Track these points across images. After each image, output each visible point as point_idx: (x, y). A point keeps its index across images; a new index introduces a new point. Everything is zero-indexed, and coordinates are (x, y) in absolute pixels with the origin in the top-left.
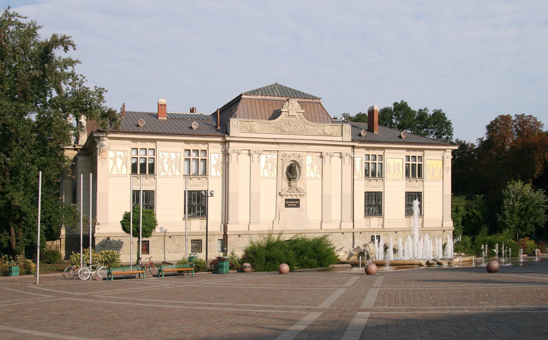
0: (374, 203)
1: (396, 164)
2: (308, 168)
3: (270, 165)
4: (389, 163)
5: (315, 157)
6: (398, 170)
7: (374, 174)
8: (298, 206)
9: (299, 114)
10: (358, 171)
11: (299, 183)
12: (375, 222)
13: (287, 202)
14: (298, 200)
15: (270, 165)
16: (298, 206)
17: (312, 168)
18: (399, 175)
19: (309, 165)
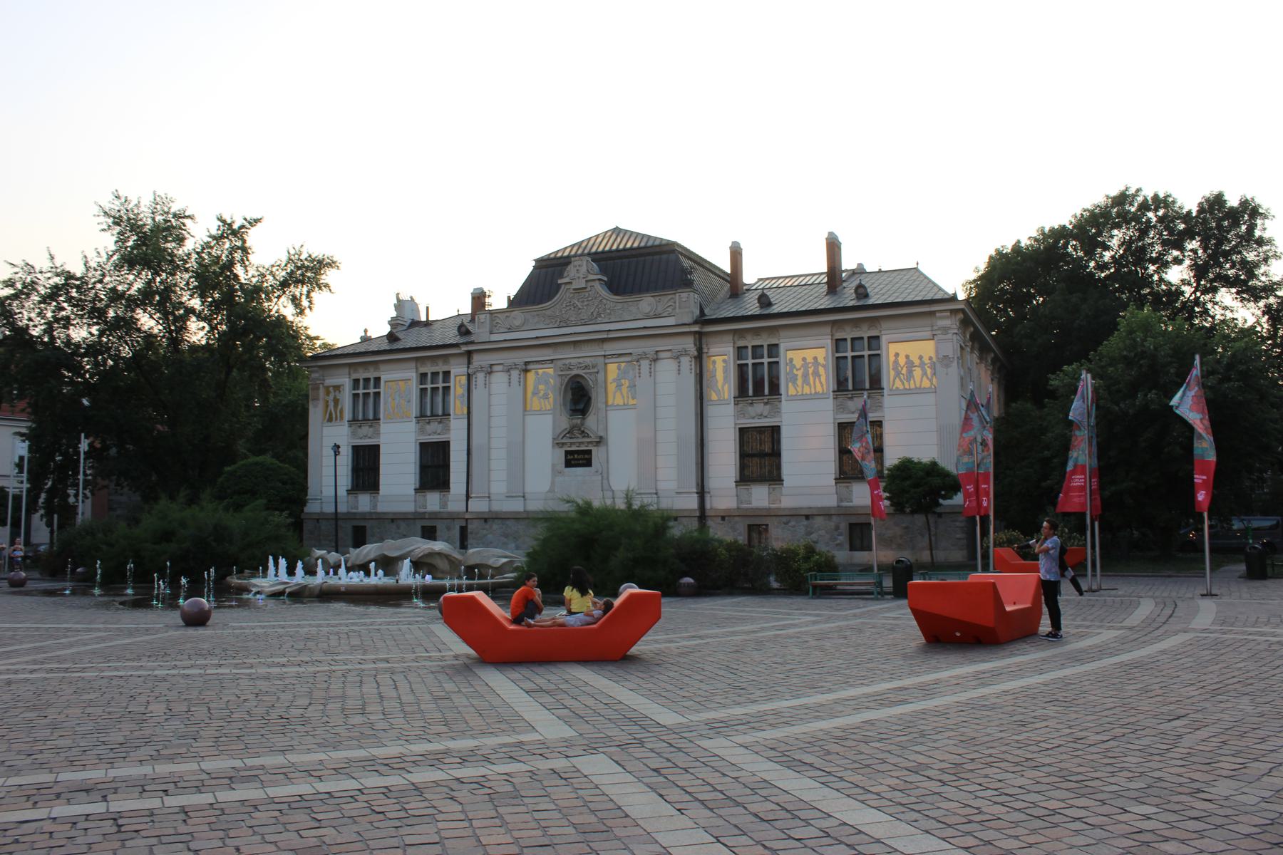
0: (761, 455)
1: (810, 360)
2: (612, 387)
3: (541, 387)
4: (791, 360)
6: (816, 374)
7: (758, 390)
8: (588, 463)
10: (720, 385)
11: (591, 421)
12: (760, 496)
14: (590, 452)
15: (541, 387)
16: (588, 463)
17: (619, 386)
19: (614, 380)
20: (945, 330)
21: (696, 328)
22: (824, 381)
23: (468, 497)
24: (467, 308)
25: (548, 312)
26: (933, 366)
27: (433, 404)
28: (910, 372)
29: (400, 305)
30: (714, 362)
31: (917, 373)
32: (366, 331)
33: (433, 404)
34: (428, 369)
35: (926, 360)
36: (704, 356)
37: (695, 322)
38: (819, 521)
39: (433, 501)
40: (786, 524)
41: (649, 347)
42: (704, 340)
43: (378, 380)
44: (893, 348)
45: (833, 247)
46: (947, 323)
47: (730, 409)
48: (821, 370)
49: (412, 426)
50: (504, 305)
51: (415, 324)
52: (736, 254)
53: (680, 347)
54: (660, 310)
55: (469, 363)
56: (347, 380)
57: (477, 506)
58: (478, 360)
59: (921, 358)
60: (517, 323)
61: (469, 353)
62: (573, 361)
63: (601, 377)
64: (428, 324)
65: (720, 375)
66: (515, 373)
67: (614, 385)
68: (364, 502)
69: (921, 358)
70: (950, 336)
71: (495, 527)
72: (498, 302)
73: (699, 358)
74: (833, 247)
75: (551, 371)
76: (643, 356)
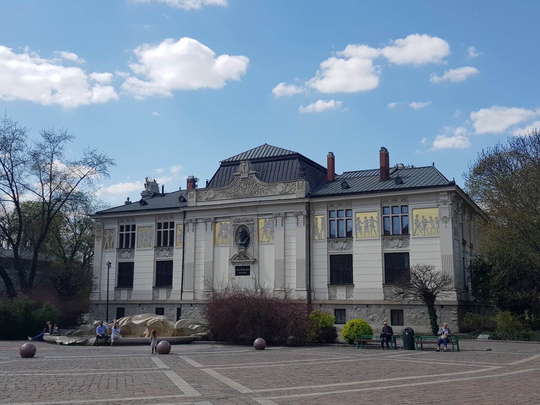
0: (342, 270)
1: (369, 218)
5: (267, 220)
8: (248, 274)
9: (251, 175)
10: (319, 232)
11: (250, 250)
13: (238, 270)
14: (249, 267)
16: (248, 274)
17: (265, 231)
18: (373, 232)
19: (263, 228)
20: (445, 202)
21: (307, 200)
22: (377, 230)
23: (182, 292)
24: (184, 187)
25: (227, 191)
26: (438, 223)
27: (165, 240)
28: (425, 225)
29: (148, 184)
30: (317, 219)
31: (429, 225)
32: (128, 199)
33: (165, 240)
34: (162, 221)
35: (434, 217)
36: (311, 215)
37: (306, 197)
38: (373, 309)
39: (162, 295)
40: (356, 309)
41: (282, 211)
42: (311, 207)
43: (134, 227)
44: (415, 212)
45: (385, 155)
46: (446, 198)
47: (325, 244)
48: (375, 224)
49: (152, 252)
50: (204, 186)
51: (156, 195)
52: (331, 159)
53: (298, 211)
54: (287, 191)
55: (184, 218)
56: (117, 226)
57: (188, 297)
58: (189, 217)
59: (431, 218)
60: (211, 196)
61: (185, 212)
62: (241, 218)
63: (256, 226)
64: (163, 195)
65: (319, 226)
66: (209, 224)
67: (262, 230)
68: (124, 295)
69: (431, 218)
70: (447, 206)
71: (196, 308)
72: (201, 185)
73: (309, 217)
74: (385, 155)
75: (229, 223)
76: (279, 215)
